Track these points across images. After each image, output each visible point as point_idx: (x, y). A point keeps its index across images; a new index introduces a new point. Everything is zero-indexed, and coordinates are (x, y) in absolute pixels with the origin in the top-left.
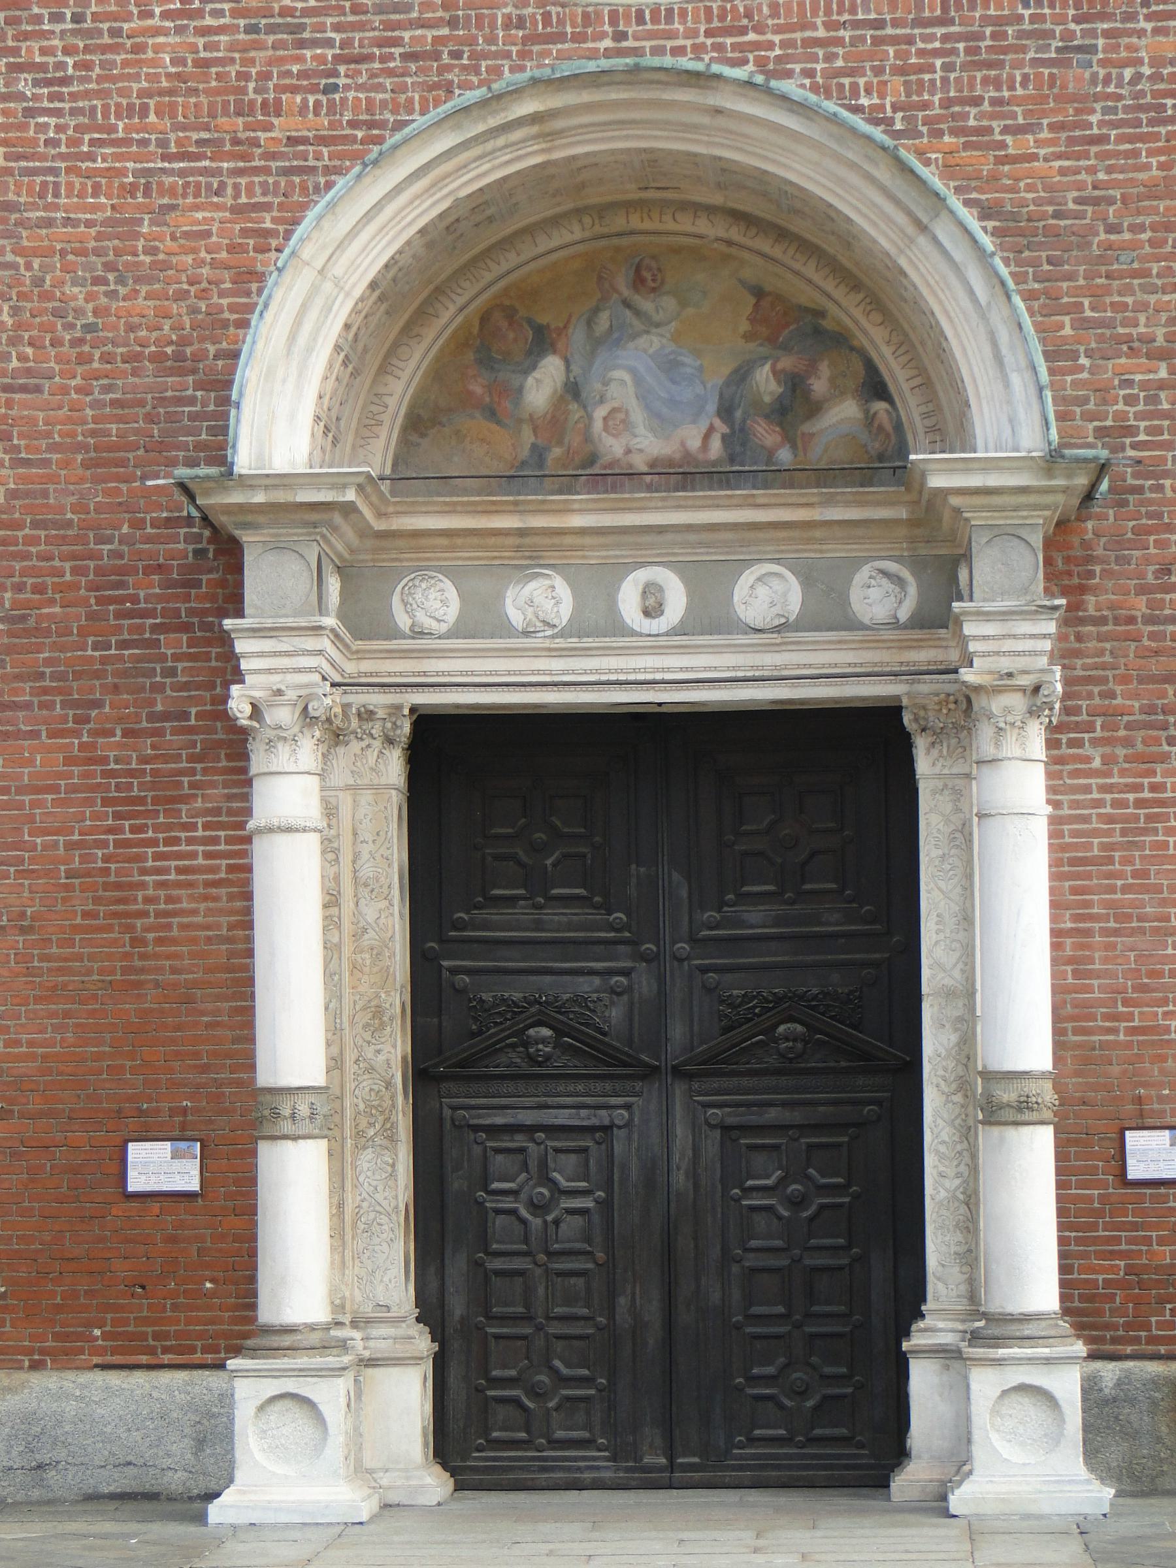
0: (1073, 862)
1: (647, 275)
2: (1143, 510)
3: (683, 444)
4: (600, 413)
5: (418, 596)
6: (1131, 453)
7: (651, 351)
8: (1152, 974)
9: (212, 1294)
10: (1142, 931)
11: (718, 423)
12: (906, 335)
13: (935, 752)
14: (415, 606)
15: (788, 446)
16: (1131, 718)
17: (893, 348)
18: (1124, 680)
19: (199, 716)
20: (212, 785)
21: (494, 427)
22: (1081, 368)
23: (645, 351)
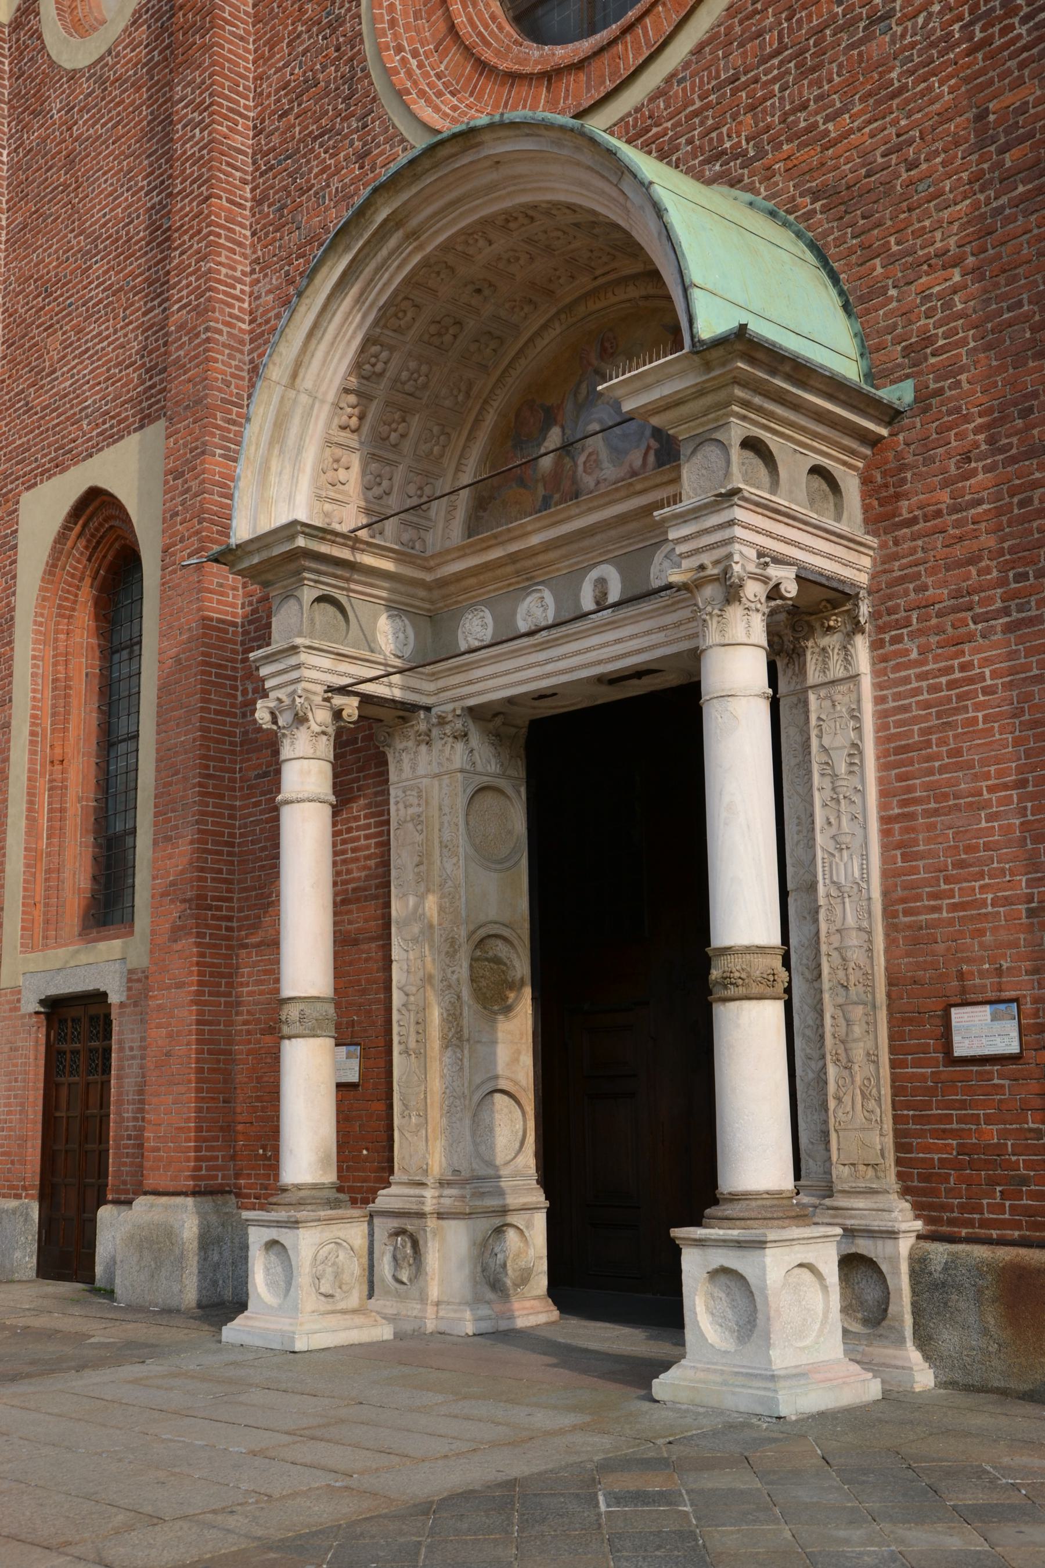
0: (898, 751)
1: (607, 345)
2: (944, 409)
3: (631, 466)
4: (581, 459)
6: (932, 360)
8: (969, 849)
9: (366, 1159)
10: (957, 808)
13: (790, 672)
16: (941, 605)
18: (932, 572)
19: (363, 740)
20: (368, 787)
22: (891, 299)
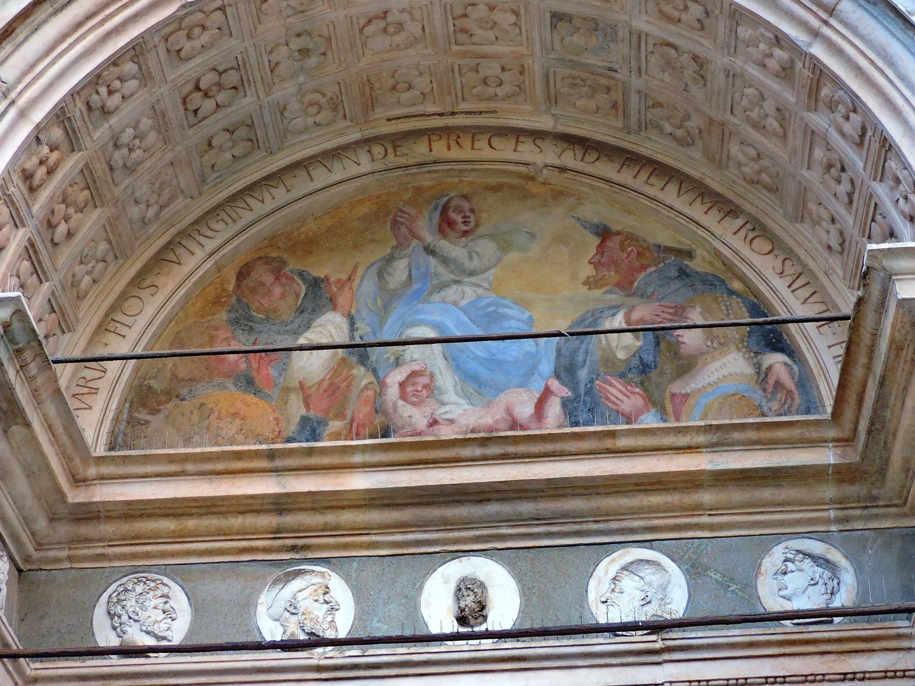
1: (458, 218)
5: (131, 604)
7: (463, 303)
11: (555, 385)
12: (804, 266)
14: (125, 618)
15: (653, 410)
17: (789, 280)
21: (250, 398)
23: (455, 304)
